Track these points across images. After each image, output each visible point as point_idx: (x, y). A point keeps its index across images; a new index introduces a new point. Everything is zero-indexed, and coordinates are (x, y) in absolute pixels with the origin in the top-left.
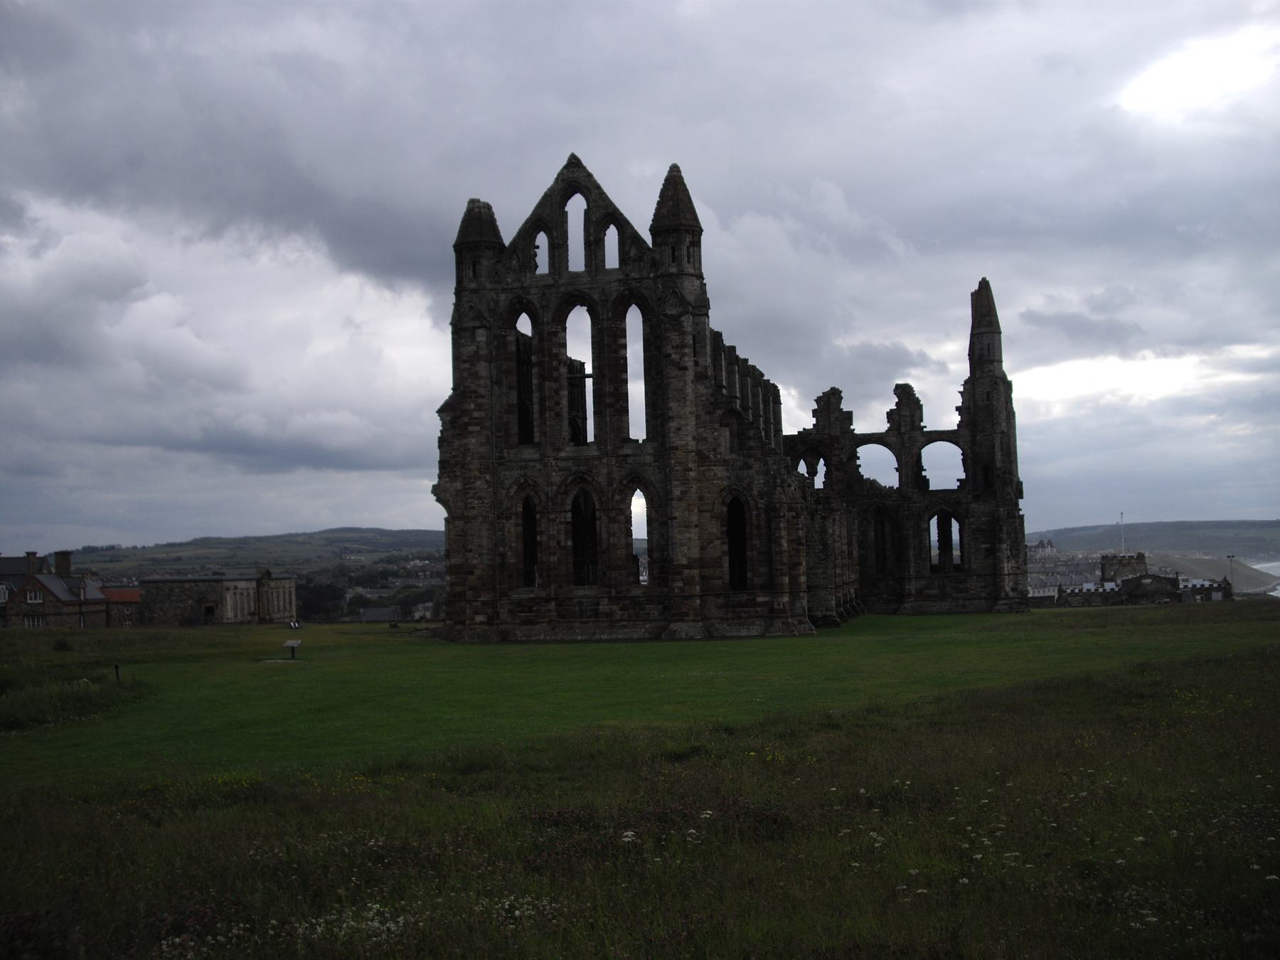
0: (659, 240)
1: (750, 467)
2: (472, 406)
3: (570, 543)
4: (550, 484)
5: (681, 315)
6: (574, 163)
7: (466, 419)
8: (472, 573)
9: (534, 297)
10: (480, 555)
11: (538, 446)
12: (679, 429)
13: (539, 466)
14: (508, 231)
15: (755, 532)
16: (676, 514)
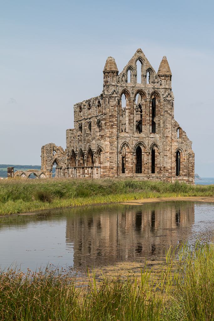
0: (163, 78)
1: (183, 143)
2: (114, 120)
3: (135, 161)
4: (132, 144)
5: (170, 100)
6: (139, 51)
7: (112, 124)
8: (113, 169)
9: (130, 90)
10: (115, 164)
11: (127, 133)
12: (169, 132)
13: (129, 138)
14: (121, 69)
15: (183, 160)
16: (168, 155)
